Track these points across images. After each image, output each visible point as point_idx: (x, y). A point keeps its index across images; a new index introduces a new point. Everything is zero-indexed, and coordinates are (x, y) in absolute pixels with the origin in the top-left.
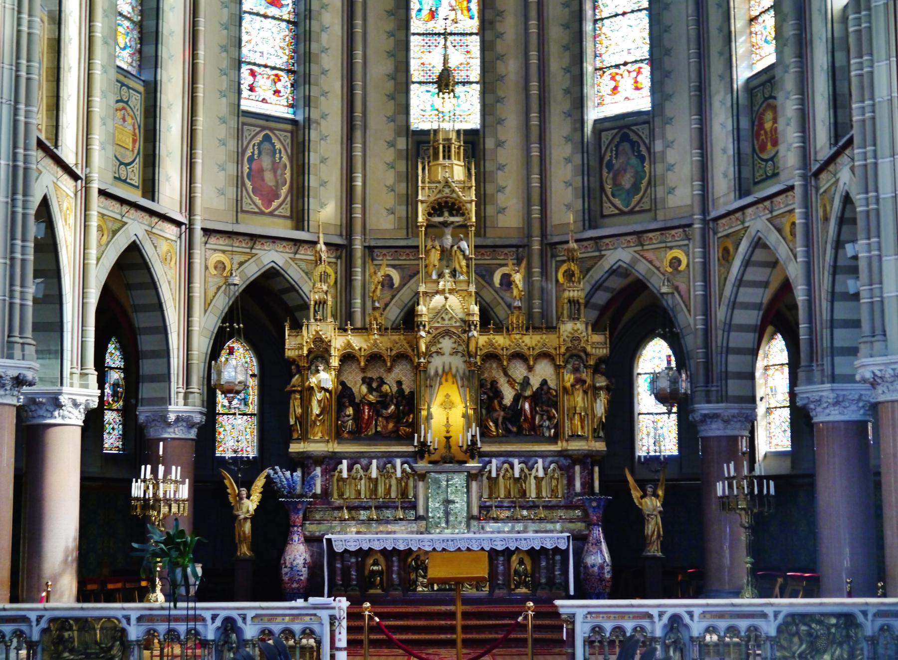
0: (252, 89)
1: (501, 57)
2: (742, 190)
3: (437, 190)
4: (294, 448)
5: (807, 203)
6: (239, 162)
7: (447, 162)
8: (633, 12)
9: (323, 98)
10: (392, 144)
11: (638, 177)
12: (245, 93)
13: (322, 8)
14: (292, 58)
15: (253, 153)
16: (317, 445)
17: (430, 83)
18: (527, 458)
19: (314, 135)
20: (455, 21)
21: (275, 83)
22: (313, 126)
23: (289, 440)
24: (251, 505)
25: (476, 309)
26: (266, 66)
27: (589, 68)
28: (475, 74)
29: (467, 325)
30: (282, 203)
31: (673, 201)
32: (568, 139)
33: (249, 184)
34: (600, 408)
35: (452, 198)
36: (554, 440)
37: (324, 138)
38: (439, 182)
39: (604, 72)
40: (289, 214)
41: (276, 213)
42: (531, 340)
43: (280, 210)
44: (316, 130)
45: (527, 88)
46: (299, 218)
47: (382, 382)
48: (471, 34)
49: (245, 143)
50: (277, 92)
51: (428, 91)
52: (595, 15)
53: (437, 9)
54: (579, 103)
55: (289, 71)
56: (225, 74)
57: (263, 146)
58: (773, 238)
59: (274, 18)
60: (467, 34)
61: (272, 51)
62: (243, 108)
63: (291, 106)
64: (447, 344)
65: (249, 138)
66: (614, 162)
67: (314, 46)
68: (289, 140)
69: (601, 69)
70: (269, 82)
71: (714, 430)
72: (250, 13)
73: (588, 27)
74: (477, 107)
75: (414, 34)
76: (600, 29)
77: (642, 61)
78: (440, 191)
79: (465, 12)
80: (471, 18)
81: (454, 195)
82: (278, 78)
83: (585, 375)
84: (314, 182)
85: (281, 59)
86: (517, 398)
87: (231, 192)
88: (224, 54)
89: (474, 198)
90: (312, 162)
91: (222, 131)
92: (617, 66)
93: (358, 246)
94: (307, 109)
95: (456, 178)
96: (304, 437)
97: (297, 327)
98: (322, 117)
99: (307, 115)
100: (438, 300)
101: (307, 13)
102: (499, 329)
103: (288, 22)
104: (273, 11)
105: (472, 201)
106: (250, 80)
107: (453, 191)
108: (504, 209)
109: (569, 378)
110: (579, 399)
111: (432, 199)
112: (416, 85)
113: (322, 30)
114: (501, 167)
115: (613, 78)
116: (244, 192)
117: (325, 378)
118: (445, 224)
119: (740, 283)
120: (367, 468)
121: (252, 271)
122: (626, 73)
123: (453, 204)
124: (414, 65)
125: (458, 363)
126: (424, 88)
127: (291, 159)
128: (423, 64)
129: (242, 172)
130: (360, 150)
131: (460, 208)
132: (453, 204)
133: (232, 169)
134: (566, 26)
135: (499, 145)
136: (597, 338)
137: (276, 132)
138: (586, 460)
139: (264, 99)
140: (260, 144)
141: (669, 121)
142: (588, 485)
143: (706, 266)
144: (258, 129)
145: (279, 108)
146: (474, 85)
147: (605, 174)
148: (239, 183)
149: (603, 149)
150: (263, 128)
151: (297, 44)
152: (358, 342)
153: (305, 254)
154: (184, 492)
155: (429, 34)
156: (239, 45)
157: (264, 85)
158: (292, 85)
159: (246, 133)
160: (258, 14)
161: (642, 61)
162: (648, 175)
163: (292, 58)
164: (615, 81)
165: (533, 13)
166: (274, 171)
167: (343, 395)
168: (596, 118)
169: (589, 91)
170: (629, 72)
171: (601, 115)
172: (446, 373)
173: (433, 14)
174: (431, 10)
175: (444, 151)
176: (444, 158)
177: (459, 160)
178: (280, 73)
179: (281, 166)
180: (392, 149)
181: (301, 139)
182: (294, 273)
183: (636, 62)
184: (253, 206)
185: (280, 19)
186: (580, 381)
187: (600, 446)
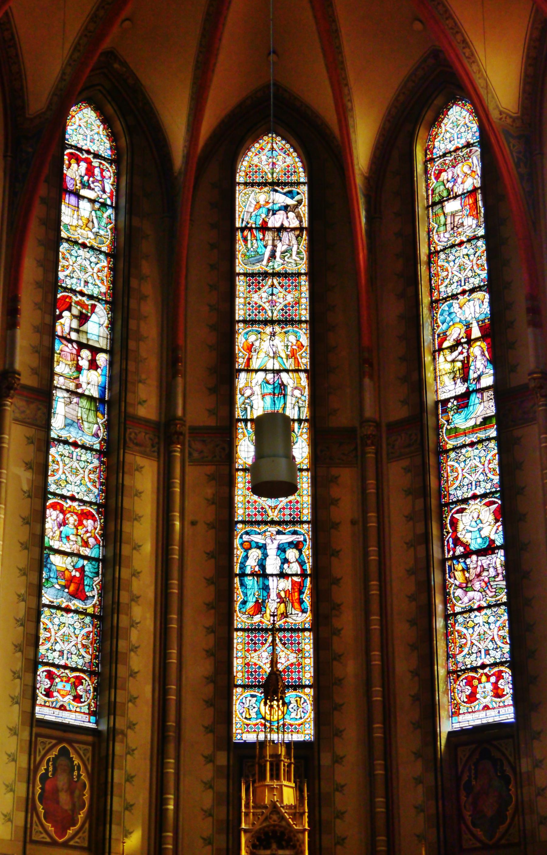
0: (48, 693)
1: (338, 657)
3: (264, 817)
6: (30, 781)
7: (275, 783)
8: (489, 607)
9: (130, 705)
10: (210, 759)
12: (41, 698)
13: (133, 600)
14: (96, 657)
15: (47, 770)
17: (255, 686)
19: (119, 748)
20: (285, 615)
21: (76, 688)
22: (119, 737)
26: (65, 667)
28: (308, 677)
32: (418, 755)
33: (41, 809)
35: (281, 827)
37: (130, 751)
38: (265, 807)
39: (459, 676)
40: (86, 845)
41: (71, 843)
43: (76, 839)
44: (122, 742)
45: (368, 694)
48: (304, 630)
49: (38, 759)
50: (77, 698)
51: (252, 696)
52: (446, 609)
53: (264, 601)
55: (91, 673)
56: (19, 677)
57: (58, 761)
59: (76, 612)
60: (298, 630)
61: (73, 650)
62: (38, 716)
63: (91, 713)
65: (43, 752)
66: (474, 783)
67: (122, 644)
68: (89, 755)
69: (455, 672)
70: (68, 687)
72: (49, 607)
73: (440, 623)
74: (310, 715)
75: (238, 630)
76: (453, 626)
77: (502, 664)
78: (266, 819)
79: (296, 605)
80: (303, 611)
81: (284, 823)
82: (79, 681)
84: (117, 805)
87: (20, 818)
88: (19, 654)
89: (307, 827)
90: (116, 780)
92: (474, 669)
94: (112, 717)
95: (286, 802)
98: (129, 727)
99: (112, 724)
101: (115, 606)
103: (93, 616)
104: (76, 604)
105: (305, 830)
106: (46, 684)
107: (283, 818)
108: (344, 839)
111: (258, 827)
112: (239, 690)
113: (132, 626)
114: (340, 788)
115: (469, 683)
116: (35, 818)
122: (484, 679)
123: (283, 834)
124: (238, 664)
126: (248, 693)
127: (91, 776)
128: (248, 664)
129: (33, 794)
130: (172, 766)
131: (290, 840)
132: (283, 834)
133: (21, 789)
134: (412, 622)
135: (337, 761)
137: (76, 745)
139: (62, 706)
140: (55, 760)
141: (537, 736)
144: (54, 742)
146: (307, 690)
147: (463, 798)
149: (460, 769)
150: (60, 740)
151: (102, 642)
155: (255, 629)
156: (36, 643)
158: (95, 689)
159: (39, 747)
160: (58, 608)
161: (502, 664)
162: (514, 799)
163: (96, 657)
164: (472, 686)
165: (375, 606)
166: (71, 791)
168: (450, 730)
170: (488, 677)
171: (457, 726)
173: (259, 607)
174: (257, 601)
175: (271, 770)
176: (272, 778)
177: (289, 780)
178: (82, 675)
179: (79, 785)
180: (210, 766)
181: (103, 753)
183: (495, 664)
184: (44, 835)
185: (84, 613)
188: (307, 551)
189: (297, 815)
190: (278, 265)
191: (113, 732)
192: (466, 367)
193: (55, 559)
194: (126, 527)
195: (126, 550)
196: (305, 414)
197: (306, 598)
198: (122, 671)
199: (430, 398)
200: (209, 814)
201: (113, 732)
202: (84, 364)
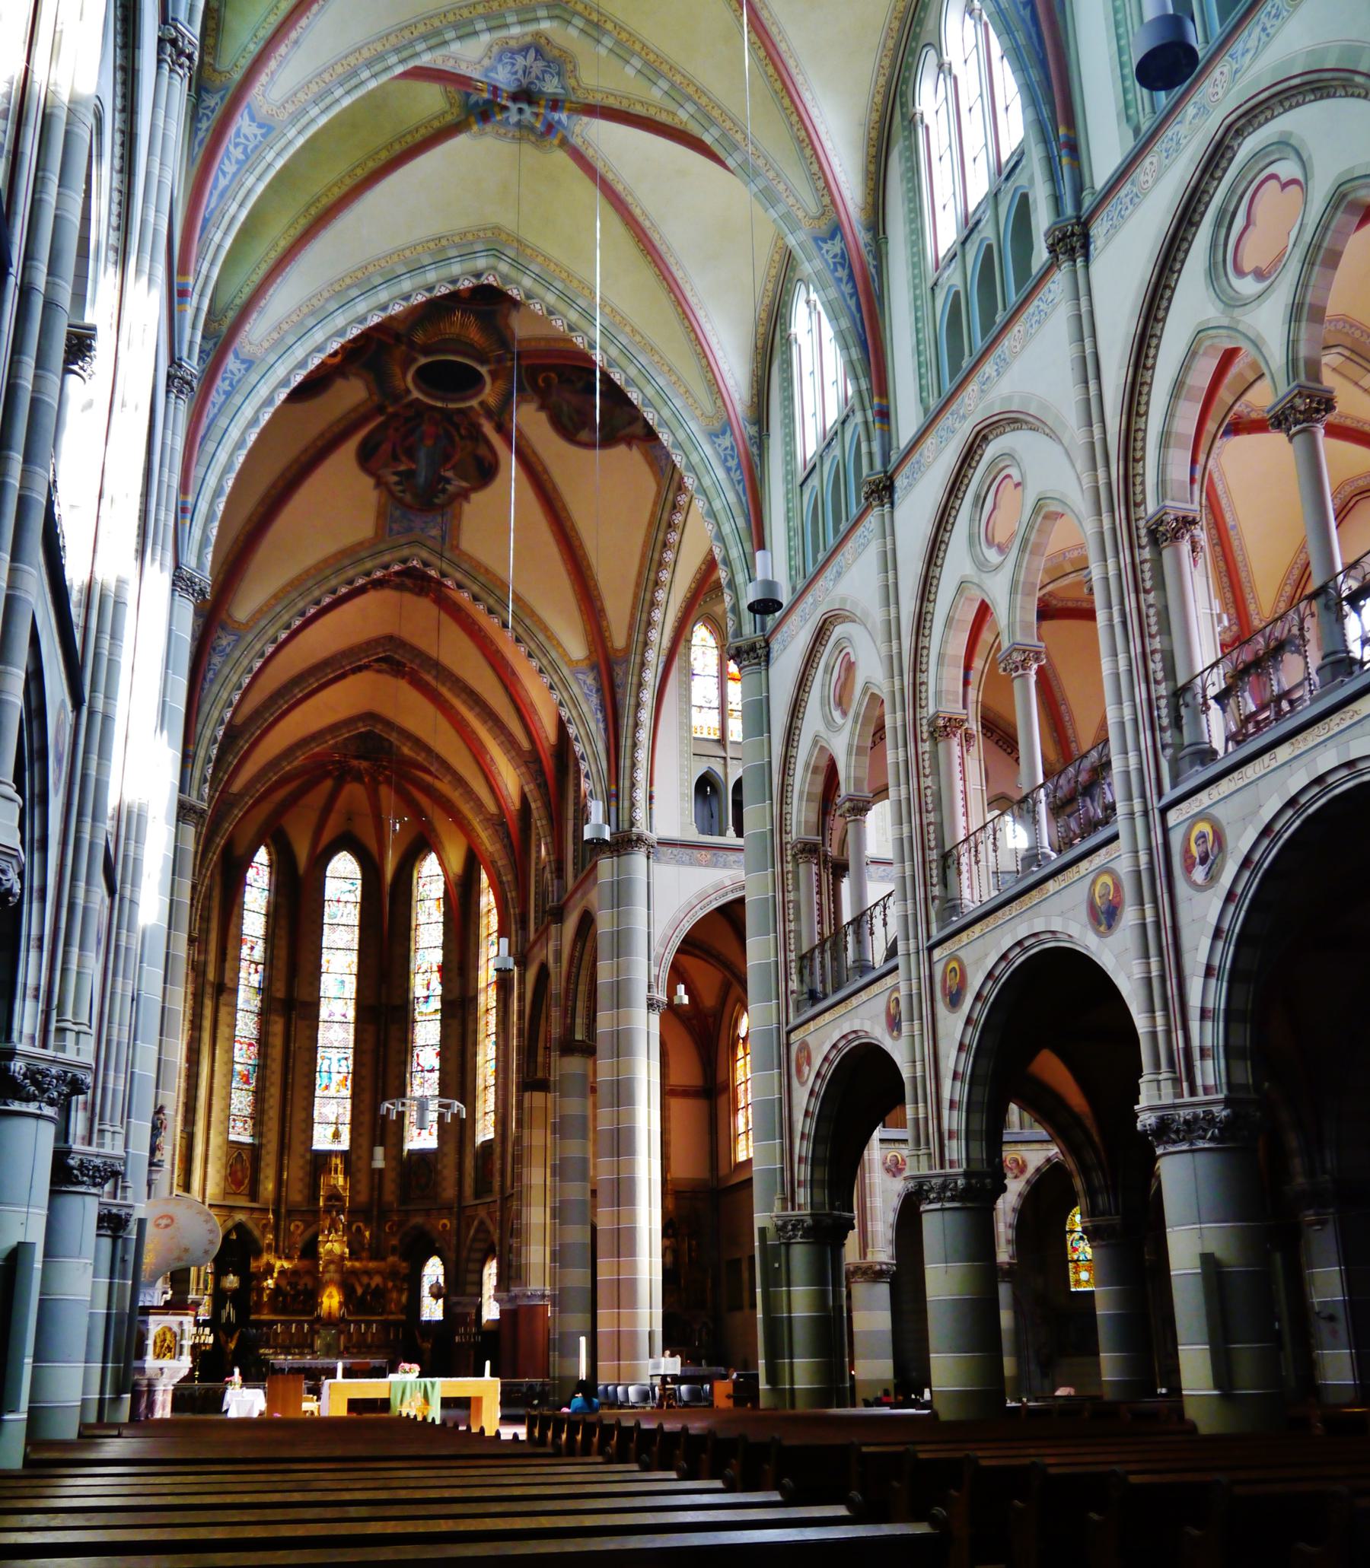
2: (477, 1196)
4: (253, 1317)
5: (502, 1210)
10: (303, 1156)
16: (265, 1317)
18: (369, 1324)
19: (263, 1152)
23: (250, 1313)
24: (232, 1346)
25: (347, 1250)
27: (407, 1122)
29: (342, 1257)
30: (245, 1187)
34: (404, 1298)
36: (381, 1314)
42: (372, 1265)
46: (254, 1195)
47: (297, 1284)
54: (401, 1140)
58: (488, 1222)
64: (332, 1267)
71: (459, 1310)
84: (262, 1176)
85: (248, 1111)
86: (364, 1293)
91: (219, 1153)
93: (283, 1210)
96: (259, 1312)
100: (329, 1246)
102: (357, 1259)
109: (390, 1284)
110: (394, 1295)
117: (270, 1283)
118: (333, 1206)
119: (474, 1240)
120: (289, 1328)
121: (230, 1224)
125: (336, 1277)
136: (404, 1265)
138: (396, 1324)
142: (396, 1335)
145: (248, 1140)
148: (226, 1179)
152: (287, 1265)
153: (256, 1215)
154: (210, 1340)
157: (239, 1124)
167: (277, 1290)
169: (406, 1134)
172: (331, 1282)
173: (327, 1087)
182: (251, 1225)
186: (395, 1286)
187: (403, 1317)
188: (351, 1062)
189: (345, 1189)
190: (343, 921)
191: (261, 1146)
192: (428, 984)
193: (238, 1067)
194: (269, 1050)
195: (269, 1062)
196: (353, 996)
197: (349, 1083)
198: (266, 1118)
200: (301, 1180)
201: (261, 1146)
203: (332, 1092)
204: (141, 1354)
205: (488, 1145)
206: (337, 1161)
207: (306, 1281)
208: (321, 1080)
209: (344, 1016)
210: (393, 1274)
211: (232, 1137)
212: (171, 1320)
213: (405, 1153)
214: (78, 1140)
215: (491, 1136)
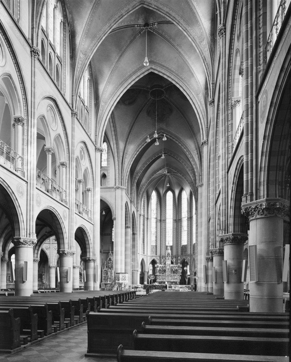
11: (186, 250)
29: (170, 264)
31: (188, 253)
34: (181, 271)
42: (175, 265)
46: (156, 255)
64: (168, 266)
83: (180, 269)
97: (156, 264)
100: (167, 262)
110: (179, 271)
117: (158, 269)
143: (190, 259)
152: (161, 266)
153: (157, 257)
167: (160, 270)
196: (172, 218)
199: (182, 217)
202: (154, 215)
203: (169, 235)
204: (119, 280)
205: (194, 244)
206: (169, 248)
207: (164, 268)
208: (167, 234)
209: (171, 222)
210: (179, 267)
211: (152, 244)
212: (124, 275)
213: (182, 245)
214: (67, 249)
215: (195, 242)
